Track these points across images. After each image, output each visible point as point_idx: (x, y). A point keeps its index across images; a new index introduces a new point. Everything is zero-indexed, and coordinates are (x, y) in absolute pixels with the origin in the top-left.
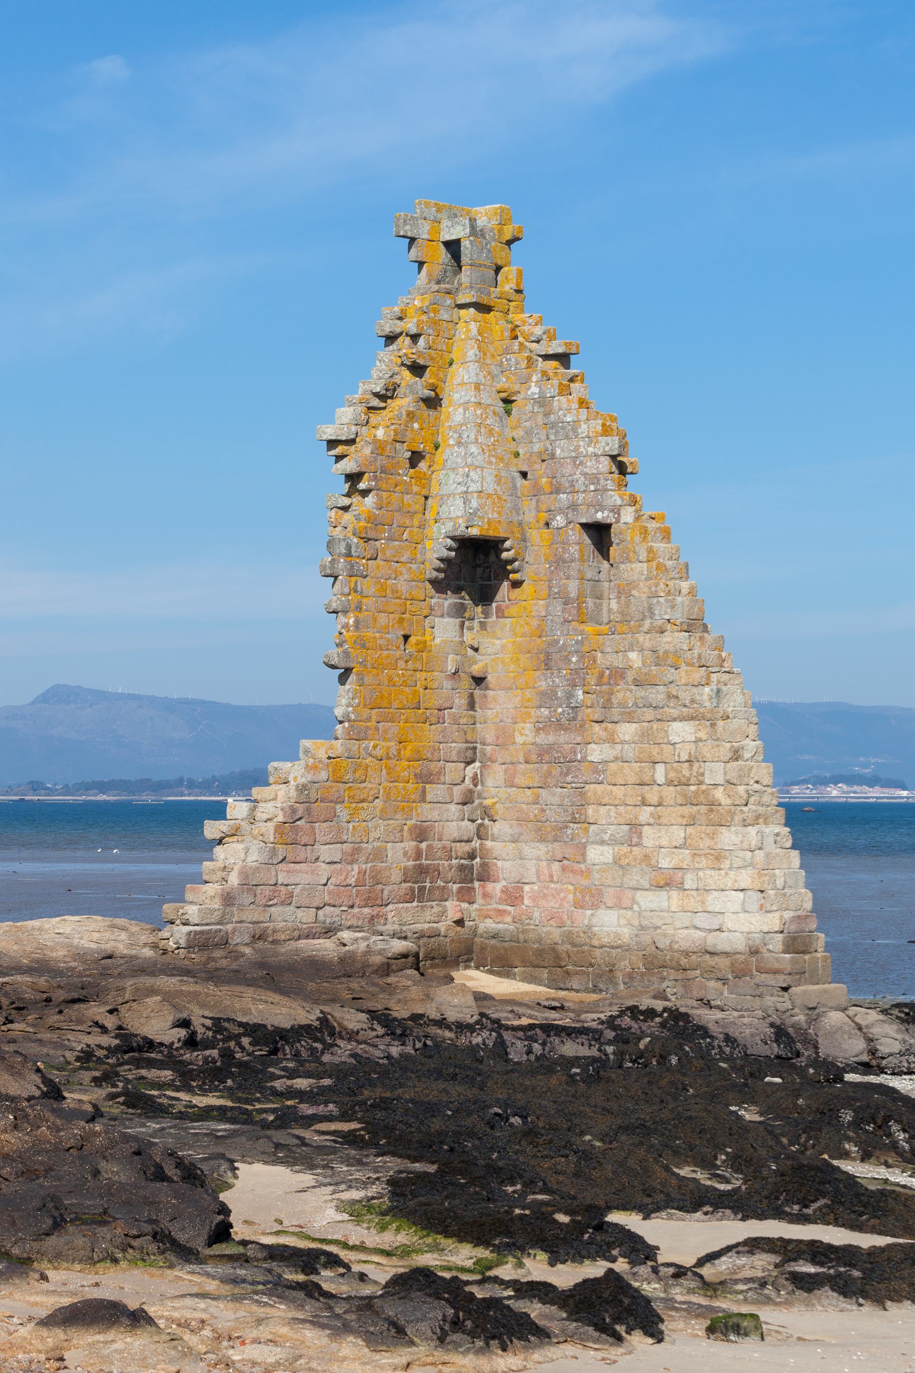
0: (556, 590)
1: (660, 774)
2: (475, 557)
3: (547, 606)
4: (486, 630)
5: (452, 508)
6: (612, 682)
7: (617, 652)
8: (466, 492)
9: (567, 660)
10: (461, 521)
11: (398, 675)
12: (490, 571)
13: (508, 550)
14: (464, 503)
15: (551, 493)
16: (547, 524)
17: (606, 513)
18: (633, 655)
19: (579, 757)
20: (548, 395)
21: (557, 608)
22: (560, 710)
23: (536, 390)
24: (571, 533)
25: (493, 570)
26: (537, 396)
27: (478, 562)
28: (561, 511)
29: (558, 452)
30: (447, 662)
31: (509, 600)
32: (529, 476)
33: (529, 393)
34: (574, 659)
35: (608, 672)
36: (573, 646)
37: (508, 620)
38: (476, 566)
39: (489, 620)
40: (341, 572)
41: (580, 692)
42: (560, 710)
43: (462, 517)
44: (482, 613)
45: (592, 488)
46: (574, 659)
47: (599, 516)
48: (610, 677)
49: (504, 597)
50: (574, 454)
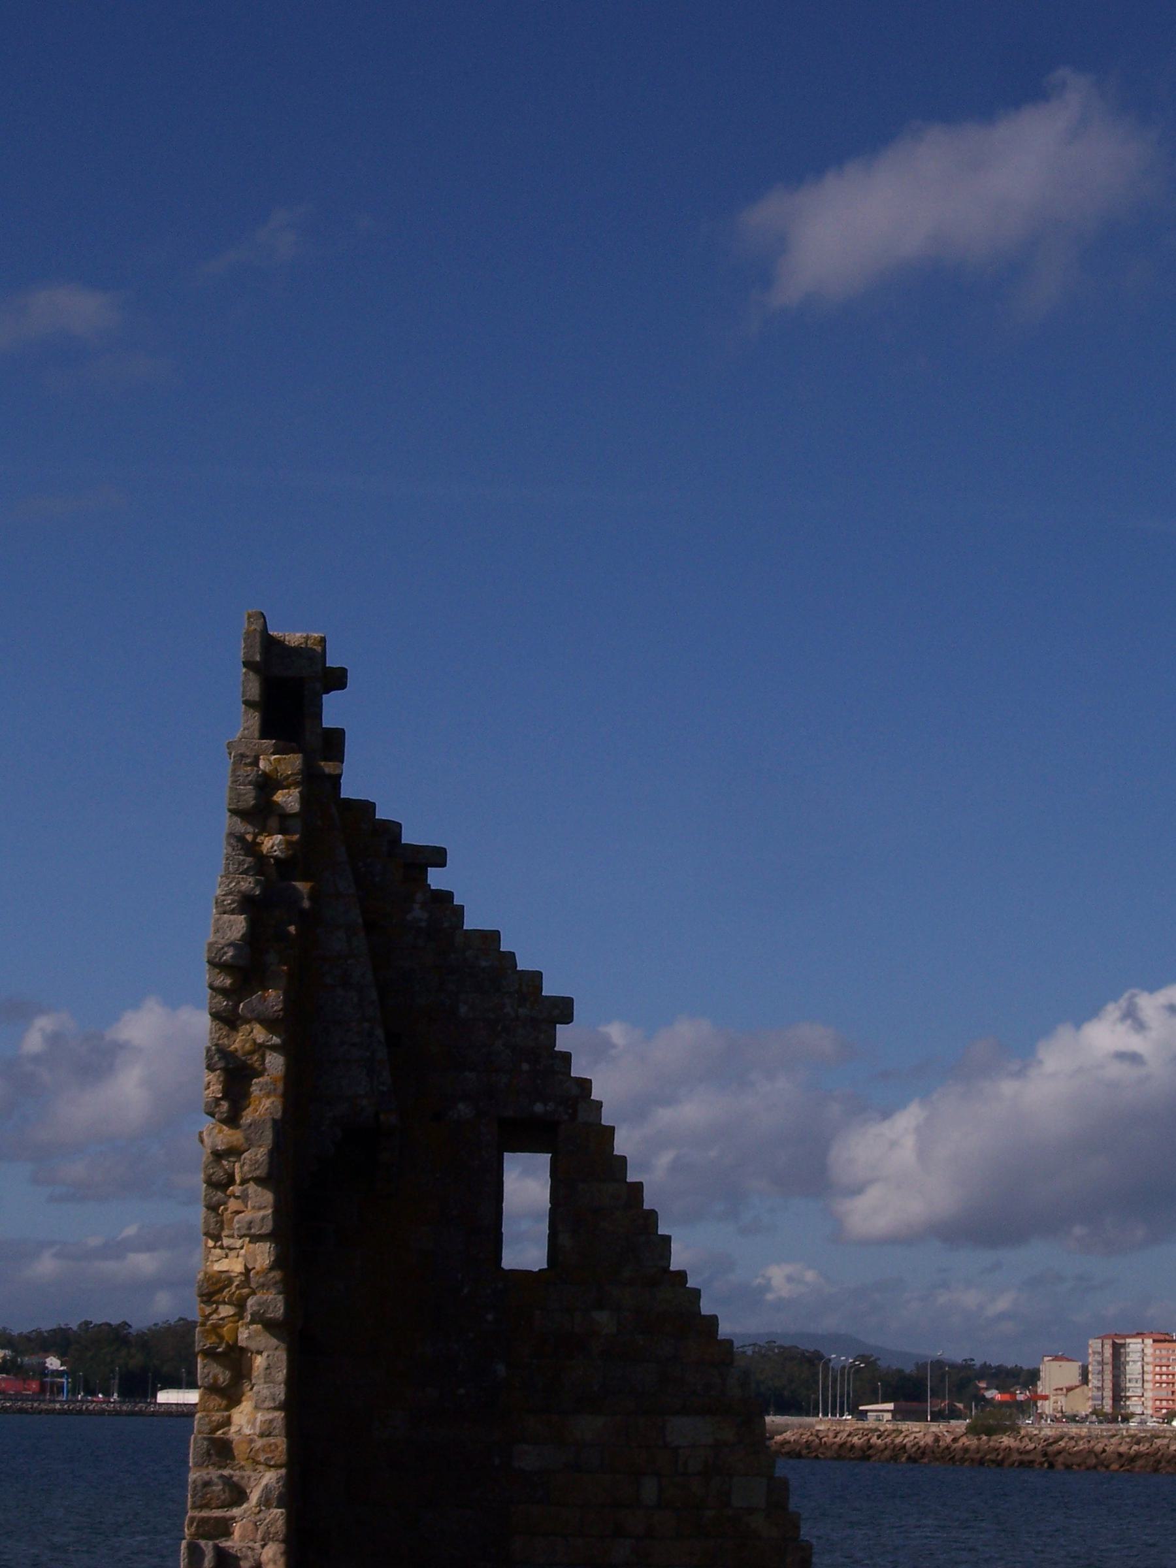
1: (649, 1490)
17: (551, 1106)
18: (603, 1318)
19: (497, 1461)
20: (446, 925)
22: (462, 1391)
23: (425, 916)
26: (423, 924)
29: (463, 1010)
33: (409, 917)
34: (490, 1317)
41: (501, 1369)
42: (462, 1391)
45: (525, 1067)
46: (490, 1317)
47: (539, 1108)
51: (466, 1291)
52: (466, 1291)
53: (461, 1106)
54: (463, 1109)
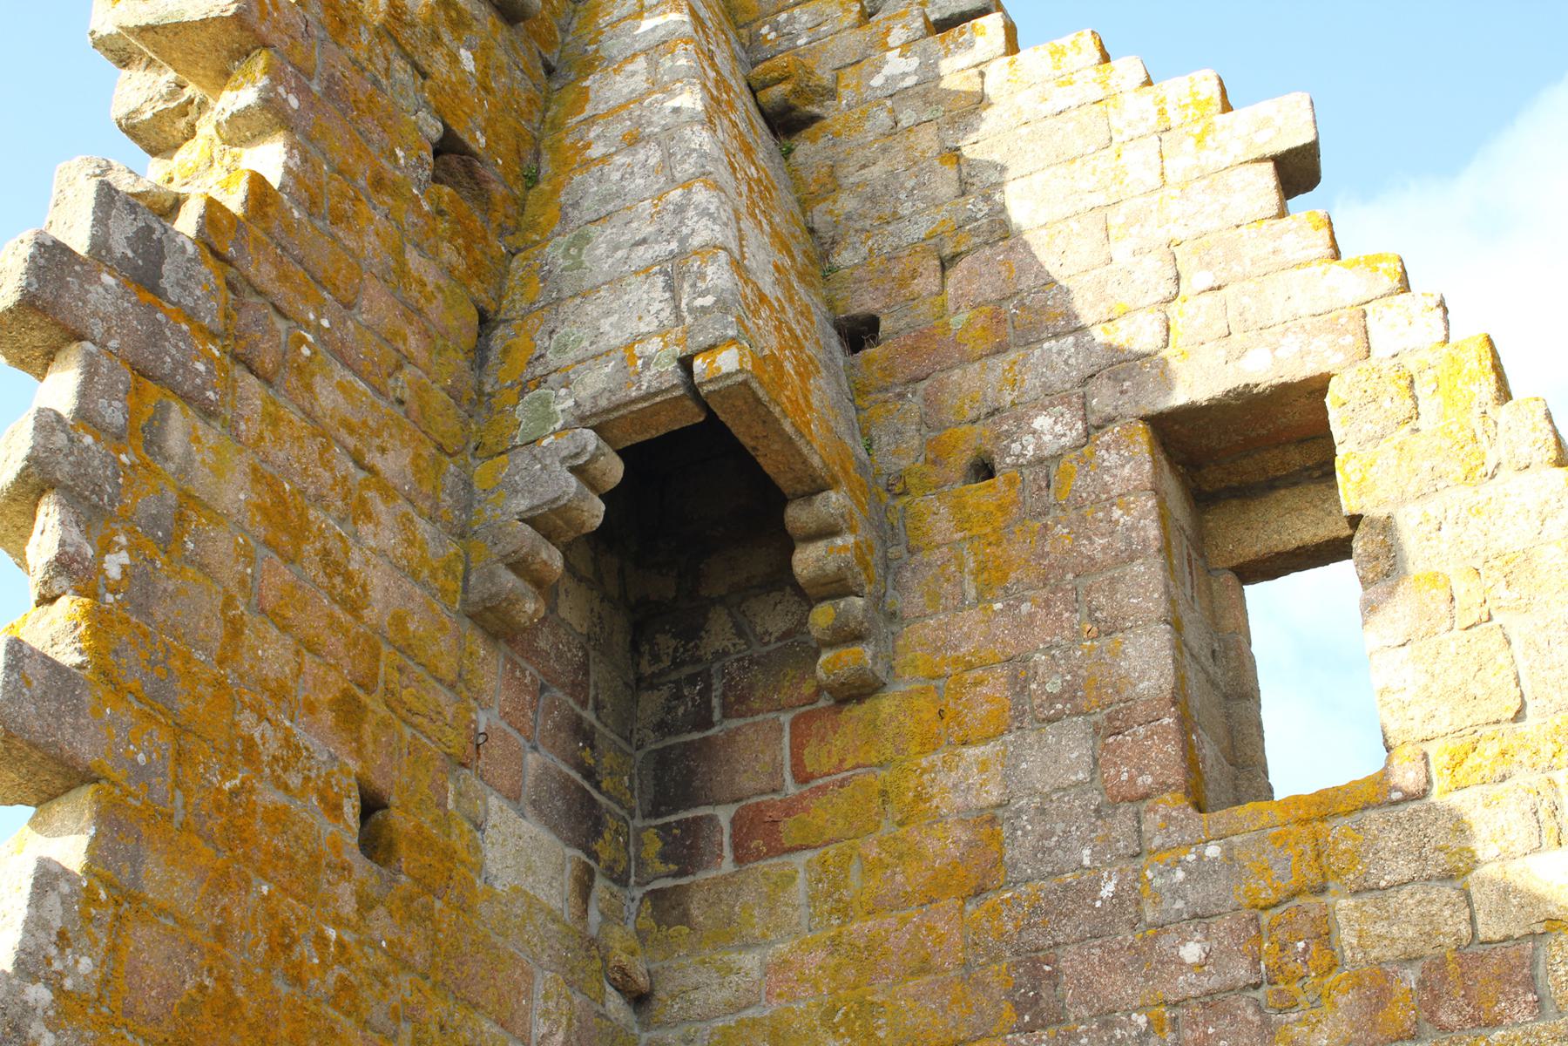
0: (1054, 686)
2: (635, 647)
3: (1009, 763)
4: (685, 918)
5: (605, 325)
6: (1445, 1016)
7: (1449, 876)
8: (680, 256)
9: (1148, 957)
10: (654, 345)
11: (321, 940)
12: (708, 688)
13: (827, 532)
14: (670, 287)
15: (1001, 349)
16: (984, 470)
21: (1065, 755)
24: (1111, 459)
25: (718, 685)
26: (910, 81)
27: (647, 668)
28: (1050, 398)
30: (528, 994)
31: (802, 777)
32: (885, 325)
33: (877, 81)
34: (1191, 952)
35: (1411, 976)
36: (1176, 892)
37: (800, 860)
38: (641, 684)
39: (701, 876)
40: (98, 330)
43: (662, 331)
44: (664, 857)
48: (1432, 991)
49: (776, 772)
50: (1099, 199)
51: (1108, 890)
52: (1108, 890)
53: (1042, 422)
54: (1051, 429)
